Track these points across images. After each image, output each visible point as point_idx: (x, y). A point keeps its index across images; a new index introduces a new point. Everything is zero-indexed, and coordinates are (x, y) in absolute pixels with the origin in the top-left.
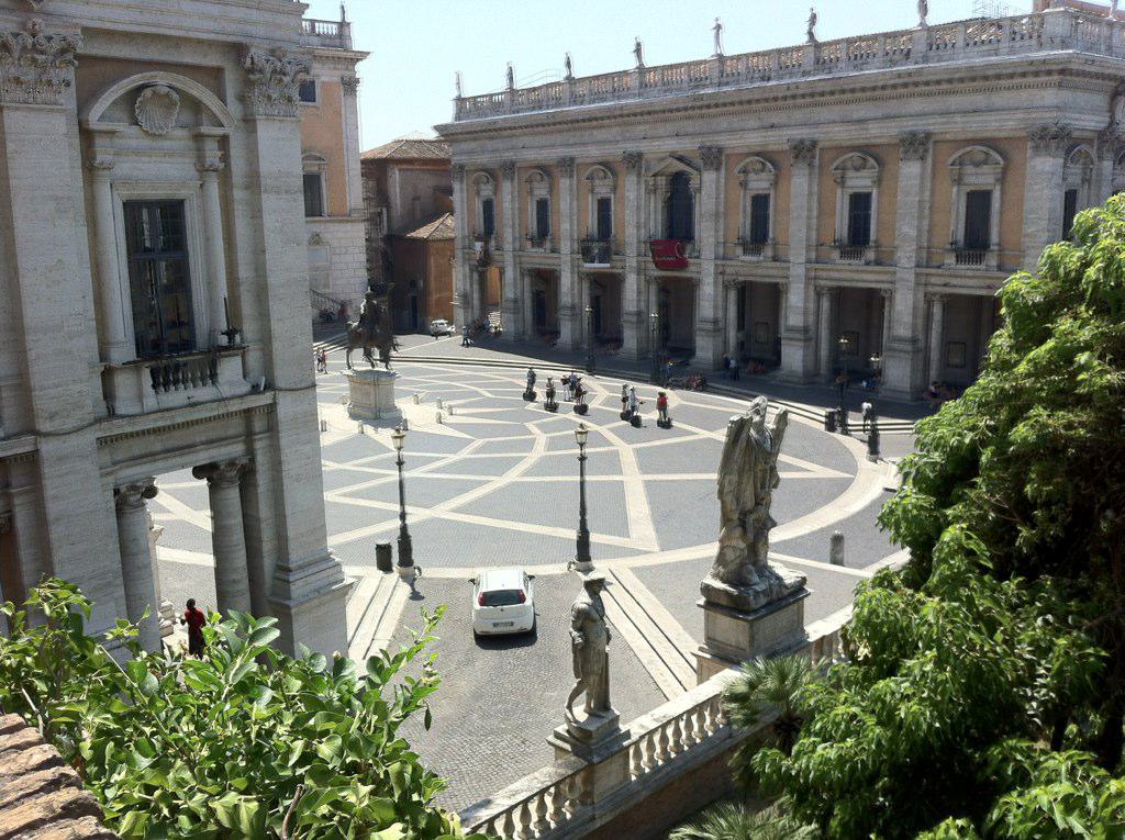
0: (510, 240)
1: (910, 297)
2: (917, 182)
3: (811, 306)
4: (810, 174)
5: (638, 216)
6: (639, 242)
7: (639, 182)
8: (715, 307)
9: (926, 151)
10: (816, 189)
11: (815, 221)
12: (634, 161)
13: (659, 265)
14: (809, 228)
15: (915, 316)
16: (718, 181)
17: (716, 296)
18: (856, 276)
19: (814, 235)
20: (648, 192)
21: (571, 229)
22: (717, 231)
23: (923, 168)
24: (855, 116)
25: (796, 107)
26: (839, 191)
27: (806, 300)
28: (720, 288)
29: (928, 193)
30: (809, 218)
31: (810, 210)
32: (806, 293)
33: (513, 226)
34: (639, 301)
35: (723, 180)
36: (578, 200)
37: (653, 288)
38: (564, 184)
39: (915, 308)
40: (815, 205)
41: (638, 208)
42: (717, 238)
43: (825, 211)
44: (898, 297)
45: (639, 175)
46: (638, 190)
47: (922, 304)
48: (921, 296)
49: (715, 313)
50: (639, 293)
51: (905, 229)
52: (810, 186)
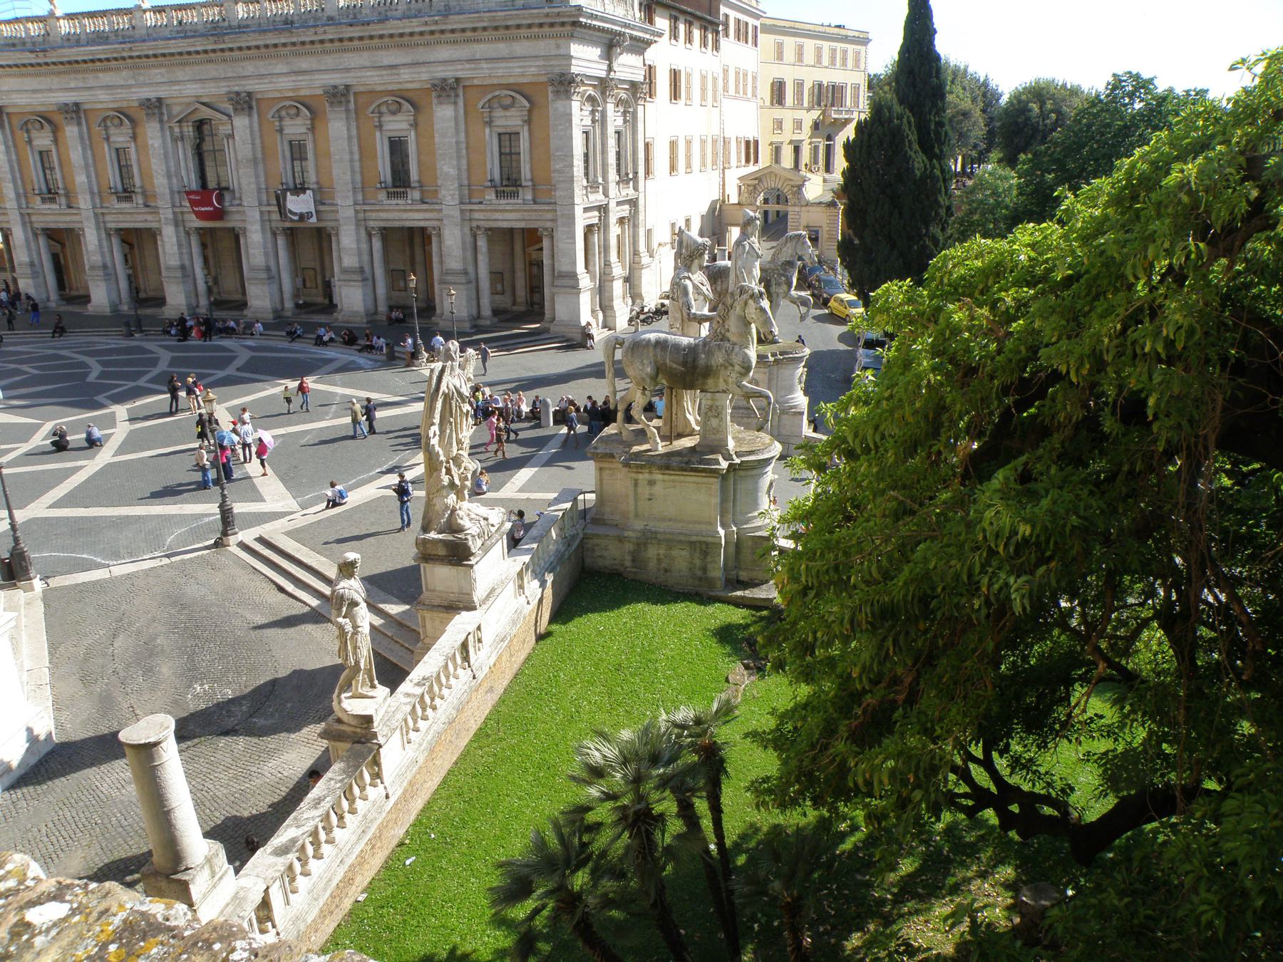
0: (12, 195)
1: (457, 232)
2: (453, 124)
3: (364, 246)
4: (347, 118)
5: (162, 162)
6: (172, 192)
7: (162, 129)
8: (266, 254)
9: (457, 96)
10: (354, 132)
11: (357, 164)
12: (155, 107)
13: (201, 216)
14: (353, 172)
15: (464, 249)
16: (251, 127)
17: (265, 242)
18: (405, 216)
19: (358, 178)
20: (175, 140)
21: (90, 182)
22: (257, 177)
23: (456, 111)
24: (386, 63)
25: (325, 52)
26: (378, 134)
27: (358, 241)
28: (269, 235)
29: (463, 135)
30: (352, 160)
31: (351, 153)
32: (358, 234)
33: (14, 180)
34: (181, 254)
35: (256, 125)
36: (92, 148)
37: (194, 240)
38: (71, 132)
39: (464, 243)
40: (356, 148)
41: (166, 155)
42: (258, 183)
43: (366, 153)
44: (447, 233)
45: (161, 121)
46: (163, 137)
47: (469, 239)
48: (467, 231)
49: (267, 260)
50: (180, 246)
51: (446, 169)
52: (348, 130)
